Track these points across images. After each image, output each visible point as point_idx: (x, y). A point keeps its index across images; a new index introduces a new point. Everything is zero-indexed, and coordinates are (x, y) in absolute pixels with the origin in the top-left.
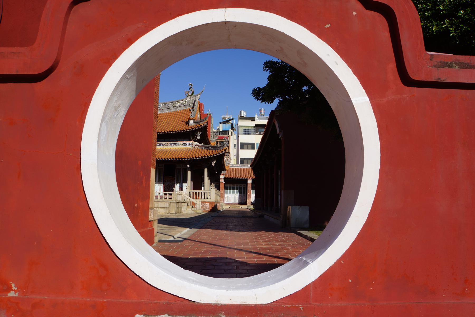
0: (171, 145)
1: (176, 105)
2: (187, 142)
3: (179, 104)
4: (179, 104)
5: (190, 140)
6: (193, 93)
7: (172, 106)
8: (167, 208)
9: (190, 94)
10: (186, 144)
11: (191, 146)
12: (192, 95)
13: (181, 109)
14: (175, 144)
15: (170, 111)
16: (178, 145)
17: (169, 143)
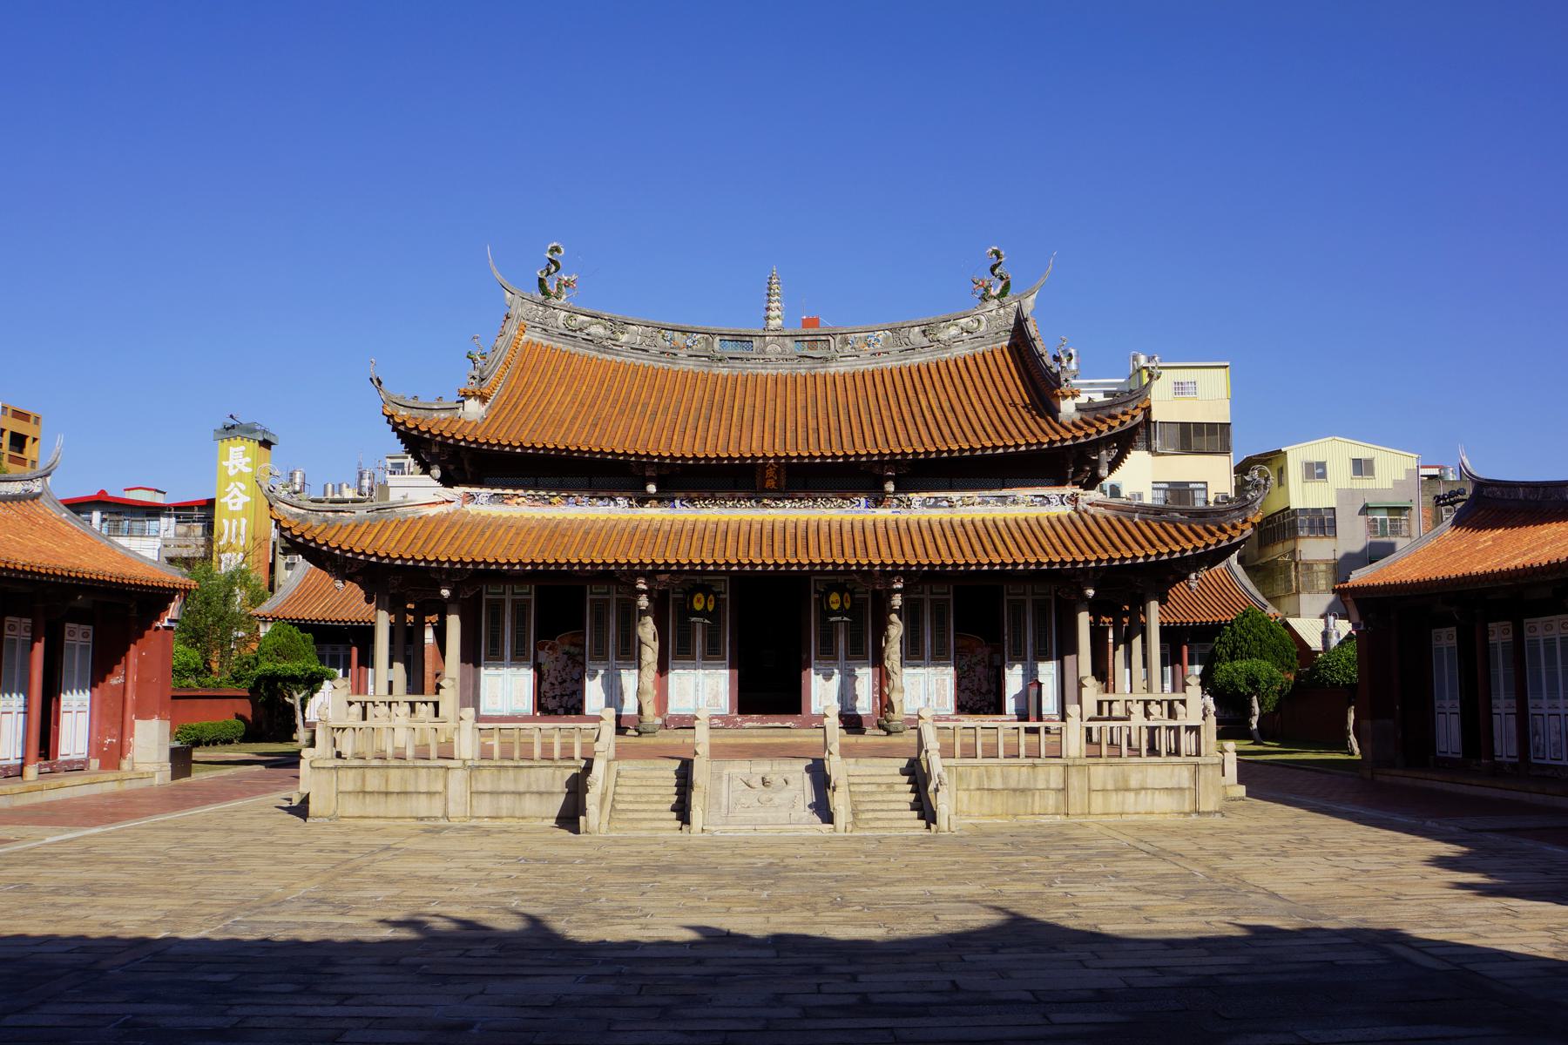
0: (984, 502)
1: (941, 336)
2: (1052, 492)
3: (953, 331)
4: (953, 331)
5: (1061, 482)
6: (1006, 287)
7: (925, 341)
8: (1181, 789)
9: (995, 292)
10: (1047, 500)
11: (1068, 509)
12: (1003, 293)
13: (961, 351)
14: (1002, 499)
15: (917, 359)
16: (1015, 502)
17: (975, 495)
